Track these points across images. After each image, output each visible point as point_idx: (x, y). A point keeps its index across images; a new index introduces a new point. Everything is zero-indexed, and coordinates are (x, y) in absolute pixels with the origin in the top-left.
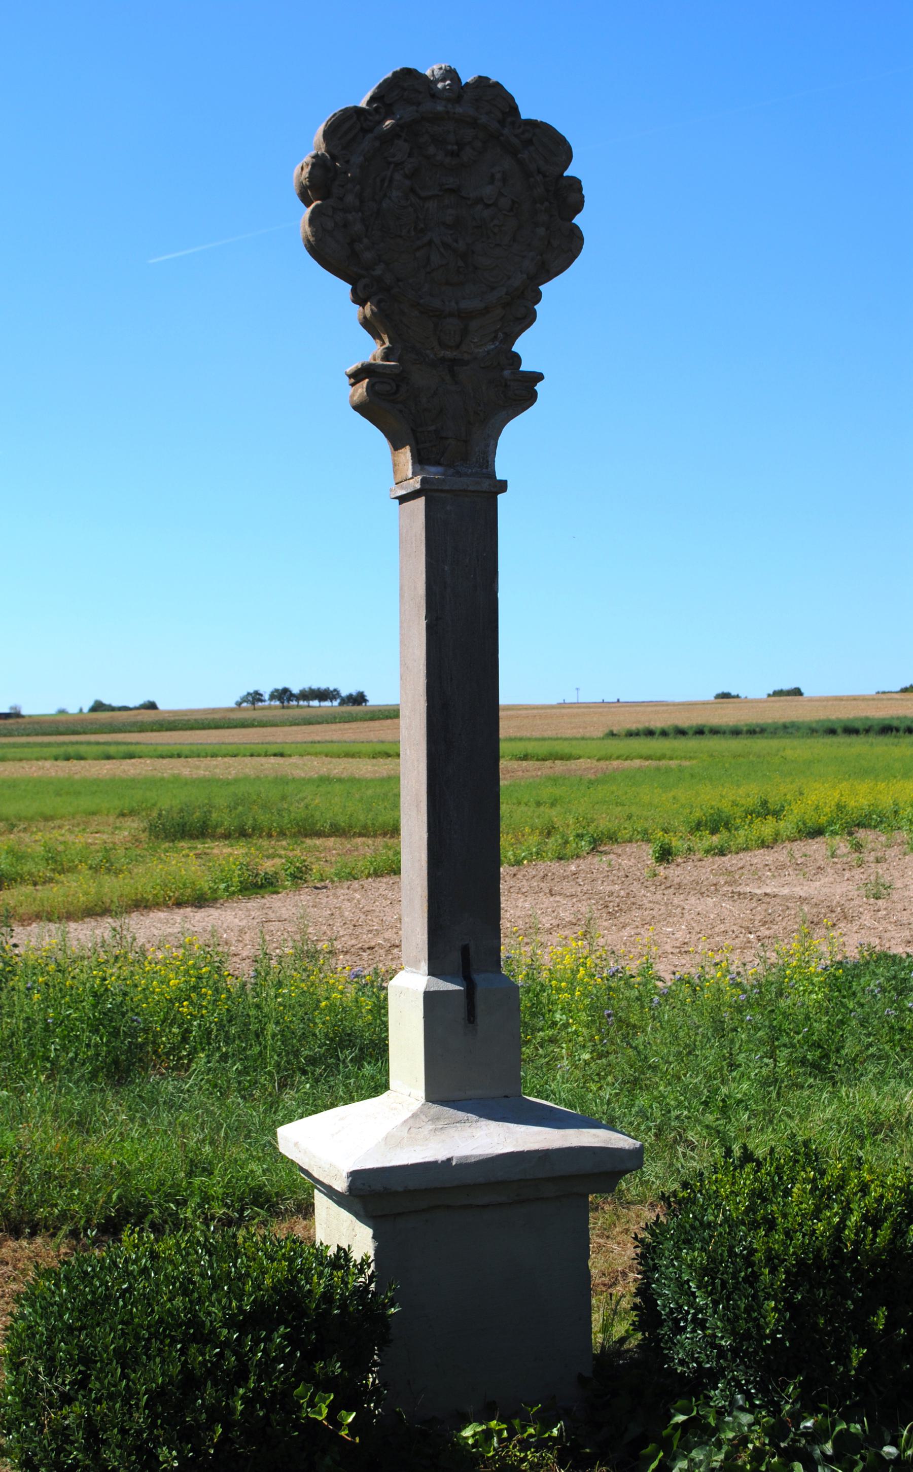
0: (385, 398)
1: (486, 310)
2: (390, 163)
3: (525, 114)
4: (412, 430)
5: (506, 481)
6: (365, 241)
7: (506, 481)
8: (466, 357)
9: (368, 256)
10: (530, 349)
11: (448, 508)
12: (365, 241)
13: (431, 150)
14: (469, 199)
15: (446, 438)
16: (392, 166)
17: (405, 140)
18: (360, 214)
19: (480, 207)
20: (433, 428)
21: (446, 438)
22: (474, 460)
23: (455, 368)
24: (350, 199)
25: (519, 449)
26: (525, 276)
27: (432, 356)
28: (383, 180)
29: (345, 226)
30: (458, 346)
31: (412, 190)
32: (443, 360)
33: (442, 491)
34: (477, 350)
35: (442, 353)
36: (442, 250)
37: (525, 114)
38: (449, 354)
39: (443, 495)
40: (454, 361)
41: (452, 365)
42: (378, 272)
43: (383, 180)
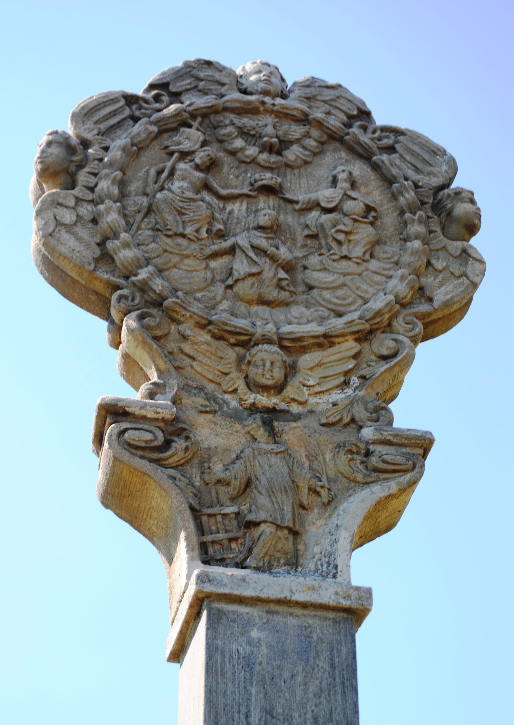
0: (148, 459)
1: (326, 341)
2: (171, 154)
3: (391, 406)
4: (192, 509)
5: (369, 592)
6: (124, 236)
7: (369, 592)
8: (295, 409)
9: (125, 255)
10: (407, 413)
11: (255, 634)
12: (124, 236)
13: (239, 143)
14: (297, 202)
15: (257, 524)
16: (176, 155)
17: (198, 129)
18: (118, 204)
19: (315, 214)
20: (231, 509)
21: (257, 524)
22: (312, 566)
23: (276, 424)
24: (104, 185)
25: (396, 575)
26: (391, 297)
27: (234, 403)
28: (159, 173)
29: (95, 221)
30: (279, 388)
31: (207, 187)
32: (253, 409)
33: (240, 600)
34: (313, 400)
35: (251, 398)
36: (252, 254)
37: (391, 406)
38: (264, 400)
39: (243, 609)
40: (273, 411)
41: (271, 416)
42: (143, 274)
43: (159, 173)
